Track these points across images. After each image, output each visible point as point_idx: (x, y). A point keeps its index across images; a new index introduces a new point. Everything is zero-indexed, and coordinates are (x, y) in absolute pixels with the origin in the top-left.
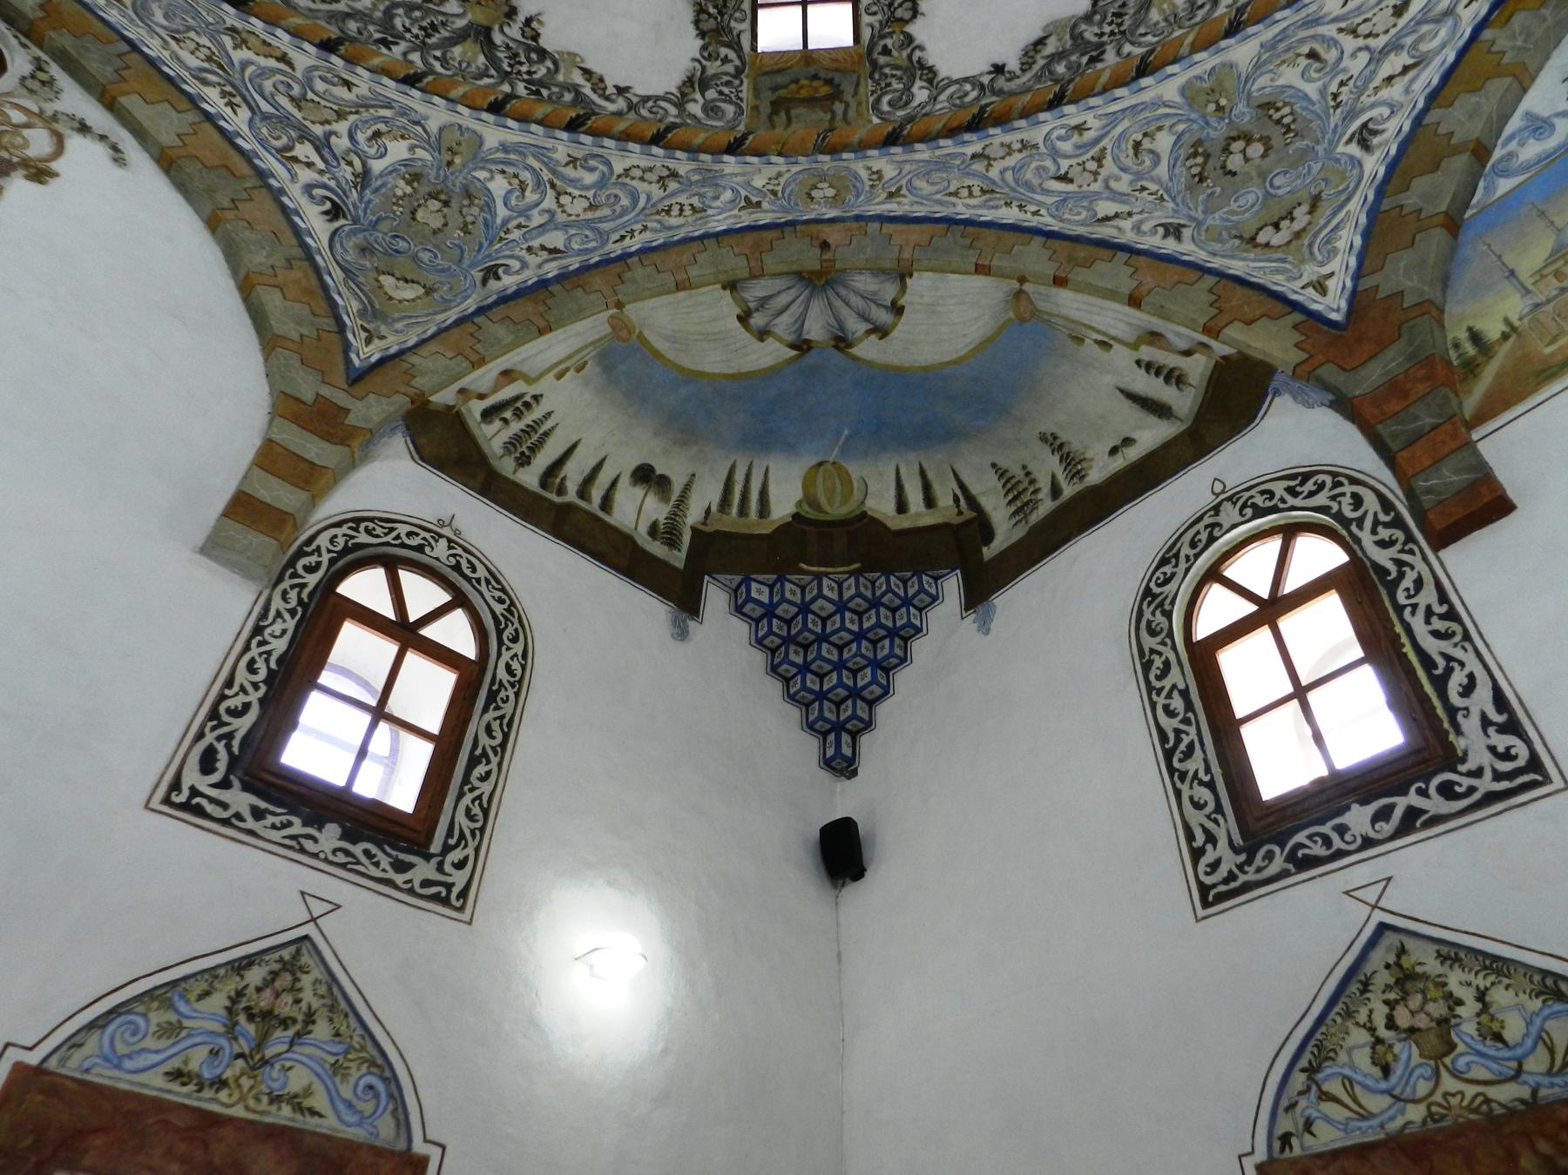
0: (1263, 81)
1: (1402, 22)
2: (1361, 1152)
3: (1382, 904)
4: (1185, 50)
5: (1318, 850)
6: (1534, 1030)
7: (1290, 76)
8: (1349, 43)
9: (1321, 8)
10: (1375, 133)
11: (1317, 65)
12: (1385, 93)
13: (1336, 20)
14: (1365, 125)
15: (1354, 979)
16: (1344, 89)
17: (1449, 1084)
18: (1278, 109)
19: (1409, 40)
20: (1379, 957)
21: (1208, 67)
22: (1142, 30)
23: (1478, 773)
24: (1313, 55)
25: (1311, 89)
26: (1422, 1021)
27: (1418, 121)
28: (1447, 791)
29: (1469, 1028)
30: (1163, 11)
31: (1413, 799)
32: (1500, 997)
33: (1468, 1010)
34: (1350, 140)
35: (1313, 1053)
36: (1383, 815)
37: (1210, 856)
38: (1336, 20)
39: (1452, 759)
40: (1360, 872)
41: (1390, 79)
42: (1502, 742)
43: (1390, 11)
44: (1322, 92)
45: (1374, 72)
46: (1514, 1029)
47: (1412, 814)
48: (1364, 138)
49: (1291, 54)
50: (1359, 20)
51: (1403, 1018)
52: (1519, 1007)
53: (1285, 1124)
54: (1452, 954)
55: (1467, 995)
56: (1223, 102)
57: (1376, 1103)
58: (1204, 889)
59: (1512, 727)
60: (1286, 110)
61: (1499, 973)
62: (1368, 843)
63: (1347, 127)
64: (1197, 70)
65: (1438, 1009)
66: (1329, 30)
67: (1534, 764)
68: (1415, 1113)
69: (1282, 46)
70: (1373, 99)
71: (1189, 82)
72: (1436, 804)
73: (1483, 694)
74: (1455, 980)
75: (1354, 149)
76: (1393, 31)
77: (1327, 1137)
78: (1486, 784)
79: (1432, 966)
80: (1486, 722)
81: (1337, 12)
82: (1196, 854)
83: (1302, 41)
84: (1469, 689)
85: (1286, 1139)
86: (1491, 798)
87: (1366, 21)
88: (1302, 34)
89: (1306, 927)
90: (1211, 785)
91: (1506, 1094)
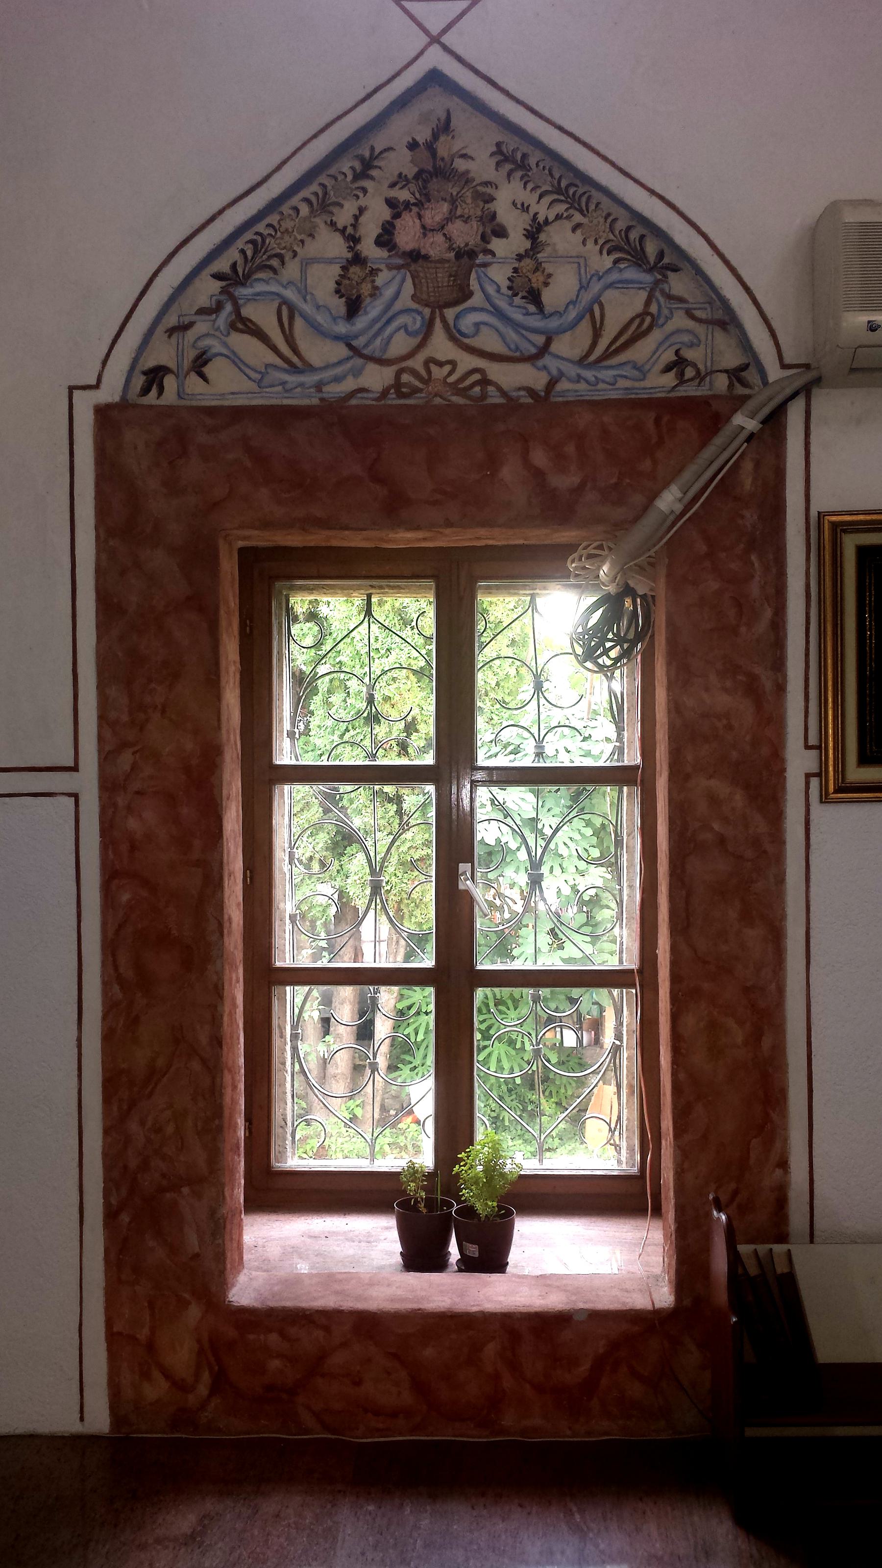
2: (280, 417)
3: (445, 39)
6: (586, 297)
15: (357, 154)
17: (440, 346)
20: (408, 126)
26: (435, 246)
29: (500, 274)
32: (561, 239)
33: (511, 245)
35: (248, 258)
46: (561, 288)
51: (408, 234)
52: (580, 261)
53: (163, 353)
54: (521, 154)
55: (515, 223)
57: (319, 352)
61: (574, 203)
65: (464, 234)
68: (376, 378)
74: (509, 199)
77: (225, 385)
79: (482, 167)
85: (155, 376)
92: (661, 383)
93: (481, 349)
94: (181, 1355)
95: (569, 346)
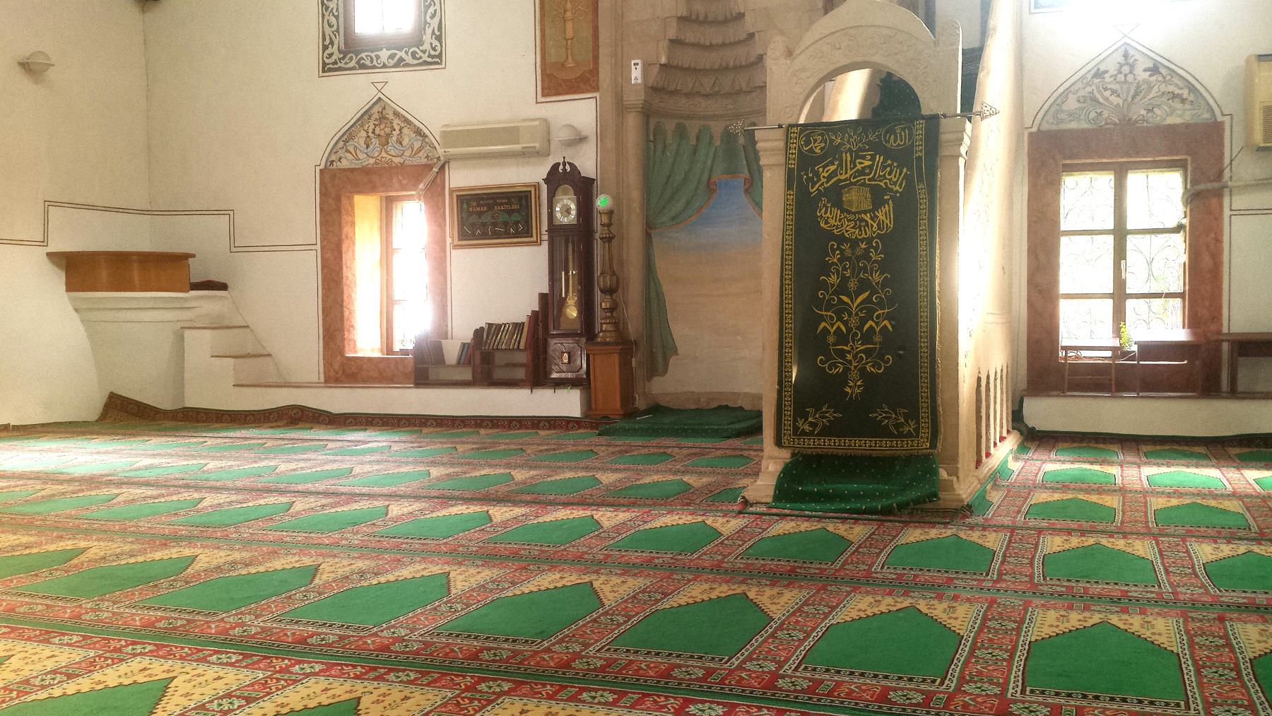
5: (368, 63)
17: (384, 154)
20: (377, 108)
23: (424, 52)
26: (382, 133)
28: (414, 54)
29: (394, 139)
31: (402, 54)
32: (405, 131)
33: (397, 132)
35: (348, 136)
36: (392, 57)
37: (329, 51)
39: (420, 43)
40: (379, 77)
42: (436, 43)
47: (401, 60)
51: (377, 132)
53: (333, 157)
54: (396, 114)
55: (397, 128)
57: (362, 156)
58: (324, 64)
59: (439, 38)
62: (384, 66)
65: (388, 130)
67: (440, 56)
68: (372, 161)
72: (409, 59)
73: (437, 20)
74: (396, 122)
77: (345, 164)
78: (425, 57)
79: (391, 116)
80: (433, 33)
82: (325, 48)
84: (433, 16)
85: (332, 162)
86: (426, 63)
89: (353, 92)
90: (337, 17)
91: (397, 160)
92: (424, 161)
93: (391, 154)
94: (336, 366)
95: (407, 153)
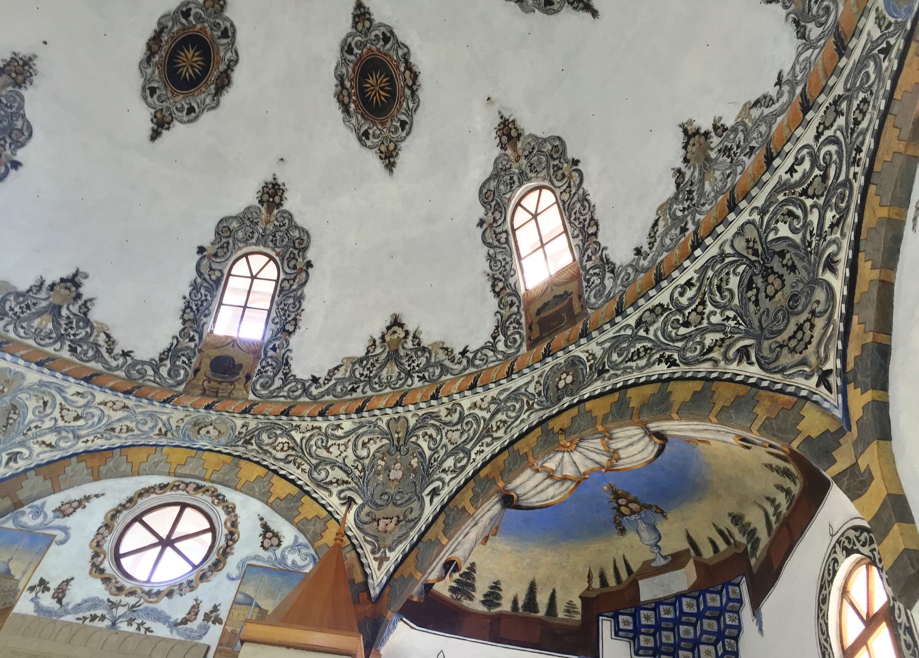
0: (24, 396)
1: (73, 424)
4: (18, 354)
7: (32, 404)
8: (57, 414)
9: (68, 387)
10: (15, 461)
11: (41, 409)
12: (36, 446)
13: (65, 398)
14: (18, 453)
16: (34, 430)
18: (15, 413)
19: (64, 434)
21: (18, 369)
22: (24, 325)
24: (45, 403)
25: (30, 416)
27: (26, 471)
30: (41, 323)
34: (8, 454)
38: (65, 398)
41: (44, 442)
43: (75, 415)
44: (31, 422)
45: (45, 434)
48: (13, 457)
49: (40, 395)
50: (68, 407)
56: (6, 390)
60: (15, 417)
63: (15, 447)
64: (13, 367)
66: (59, 399)
69: (44, 388)
70: (32, 445)
71: (6, 368)
75: (5, 458)
76: (67, 424)
81: (68, 396)
83: (50, 394)
87: (68, 410)
88: (53, 392)
